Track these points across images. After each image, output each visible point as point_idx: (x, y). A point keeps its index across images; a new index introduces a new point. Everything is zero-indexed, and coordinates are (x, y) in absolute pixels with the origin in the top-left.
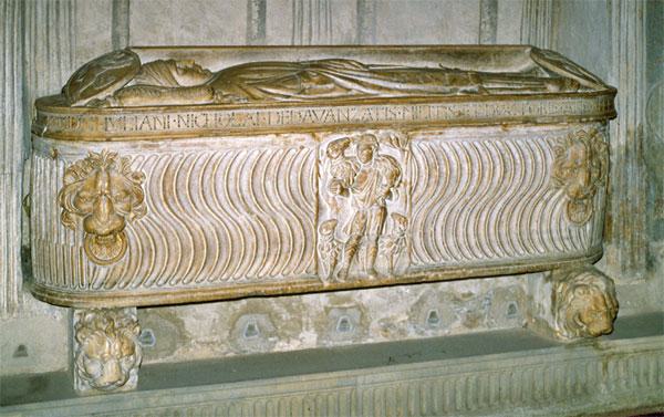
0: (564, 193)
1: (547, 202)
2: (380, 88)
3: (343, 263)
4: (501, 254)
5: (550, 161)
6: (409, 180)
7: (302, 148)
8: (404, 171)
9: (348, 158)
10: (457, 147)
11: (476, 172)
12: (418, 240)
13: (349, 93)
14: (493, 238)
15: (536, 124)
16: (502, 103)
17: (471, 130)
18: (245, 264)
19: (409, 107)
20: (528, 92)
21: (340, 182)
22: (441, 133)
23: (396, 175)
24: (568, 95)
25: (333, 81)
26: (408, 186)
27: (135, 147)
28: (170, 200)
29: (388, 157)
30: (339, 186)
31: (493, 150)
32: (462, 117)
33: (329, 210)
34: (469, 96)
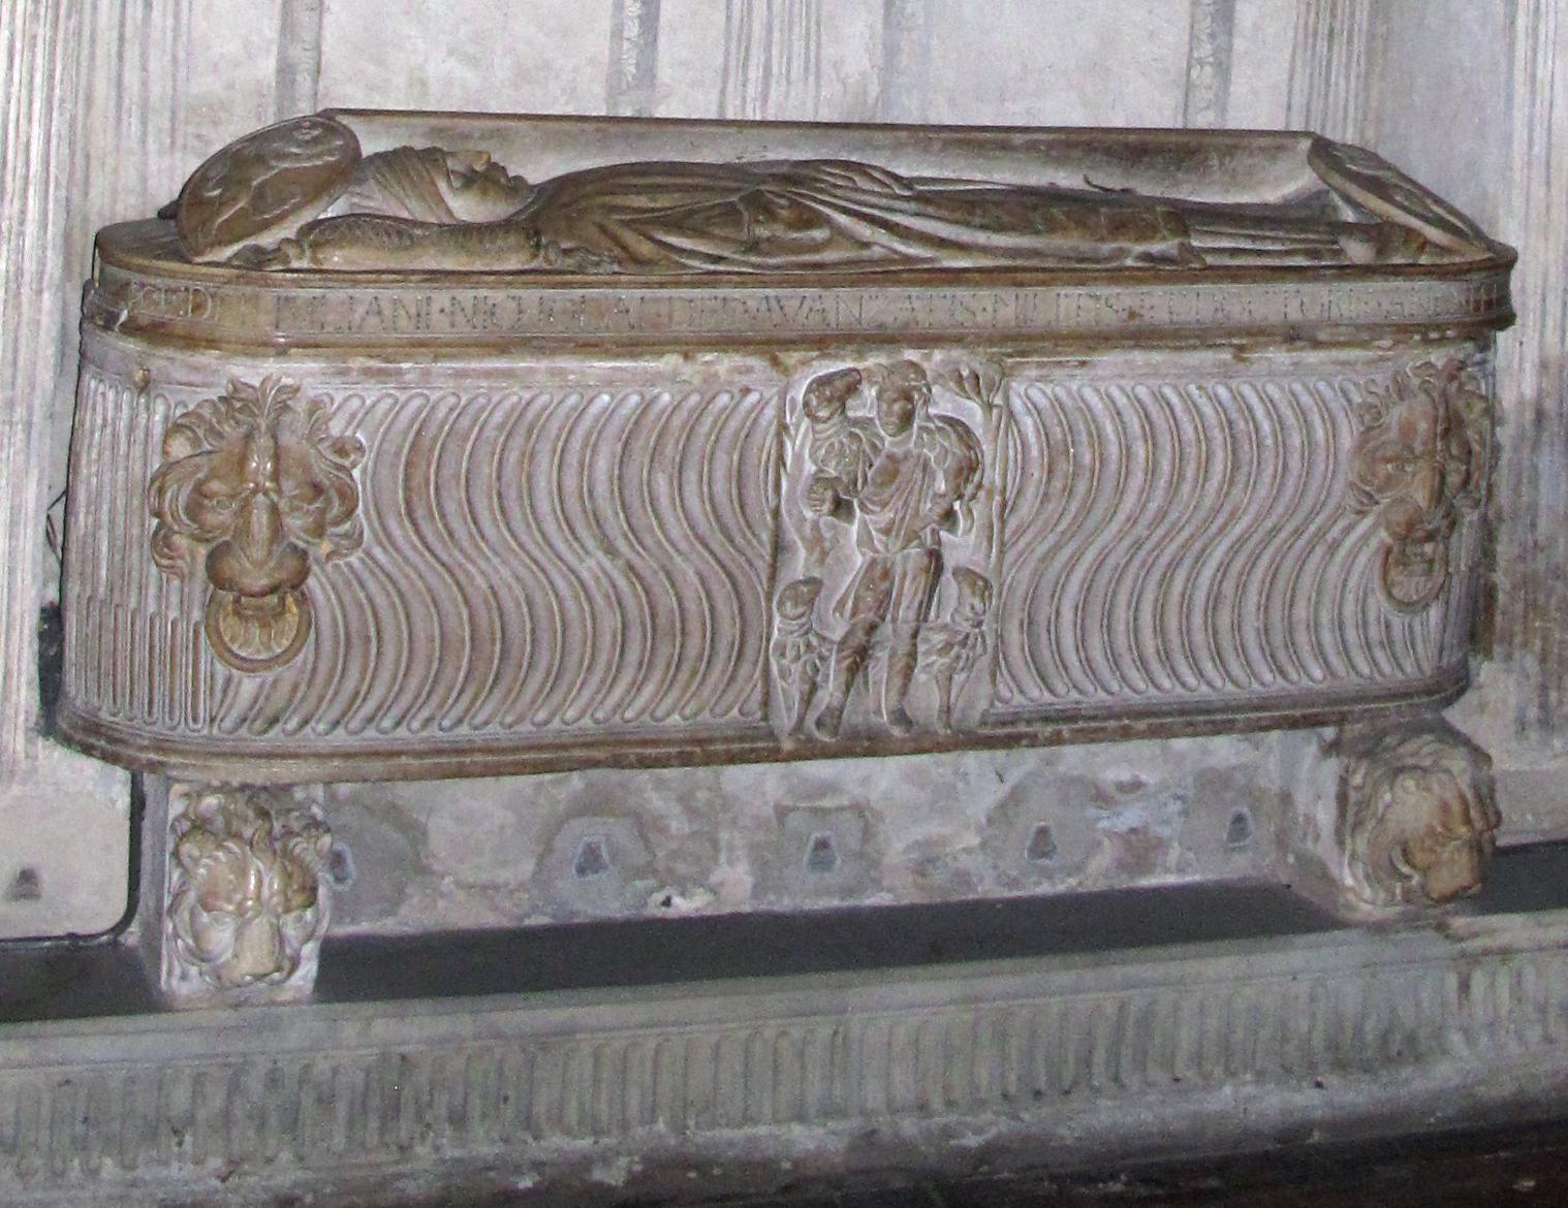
0: (1375, 526)
1: (1333, 548)
2: (942, 243)
3: (829, 693)
4: (1218, 683)
5: (1347, 441)
6: (998, 482)
7: (746, 391)
8: (988, 460)
9: (856, 422)
10: (1122, 401)
11: (1165, 466)
12: (1014, 637)
13: (866, 254)
14: (1199, 638)
15: (1317, 344)
16: (1234, 288)
17: (1157, 357)
18: (595, 680)
19: (1008, 294)
20: (1300, 261)
21: (831, 482)
22: (1083, 364)
23: (968, 468)
24: (1396, 271)
25: (827, 221)
26: (998, 498)
27: (343, 373)
28: (420, 513)
29: (952, 422)
30: (829, 494)
31: (1208, 410)
32: (1137, 322)
33: (802, 553)
34: (1156, 270)
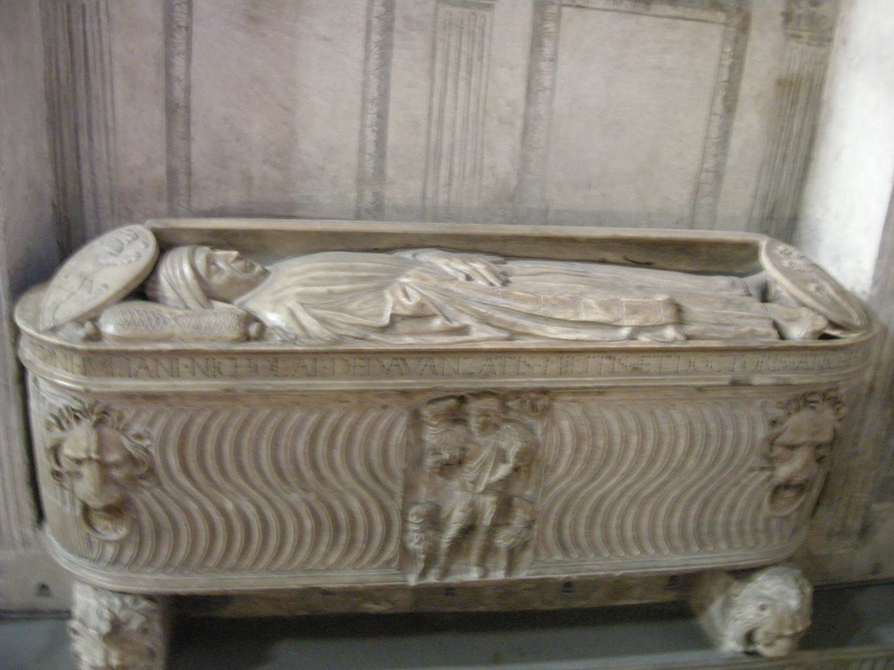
11: (649, 447)
14: (660, 531)
